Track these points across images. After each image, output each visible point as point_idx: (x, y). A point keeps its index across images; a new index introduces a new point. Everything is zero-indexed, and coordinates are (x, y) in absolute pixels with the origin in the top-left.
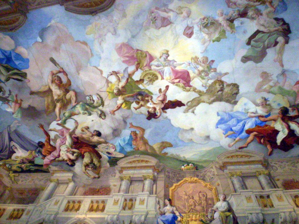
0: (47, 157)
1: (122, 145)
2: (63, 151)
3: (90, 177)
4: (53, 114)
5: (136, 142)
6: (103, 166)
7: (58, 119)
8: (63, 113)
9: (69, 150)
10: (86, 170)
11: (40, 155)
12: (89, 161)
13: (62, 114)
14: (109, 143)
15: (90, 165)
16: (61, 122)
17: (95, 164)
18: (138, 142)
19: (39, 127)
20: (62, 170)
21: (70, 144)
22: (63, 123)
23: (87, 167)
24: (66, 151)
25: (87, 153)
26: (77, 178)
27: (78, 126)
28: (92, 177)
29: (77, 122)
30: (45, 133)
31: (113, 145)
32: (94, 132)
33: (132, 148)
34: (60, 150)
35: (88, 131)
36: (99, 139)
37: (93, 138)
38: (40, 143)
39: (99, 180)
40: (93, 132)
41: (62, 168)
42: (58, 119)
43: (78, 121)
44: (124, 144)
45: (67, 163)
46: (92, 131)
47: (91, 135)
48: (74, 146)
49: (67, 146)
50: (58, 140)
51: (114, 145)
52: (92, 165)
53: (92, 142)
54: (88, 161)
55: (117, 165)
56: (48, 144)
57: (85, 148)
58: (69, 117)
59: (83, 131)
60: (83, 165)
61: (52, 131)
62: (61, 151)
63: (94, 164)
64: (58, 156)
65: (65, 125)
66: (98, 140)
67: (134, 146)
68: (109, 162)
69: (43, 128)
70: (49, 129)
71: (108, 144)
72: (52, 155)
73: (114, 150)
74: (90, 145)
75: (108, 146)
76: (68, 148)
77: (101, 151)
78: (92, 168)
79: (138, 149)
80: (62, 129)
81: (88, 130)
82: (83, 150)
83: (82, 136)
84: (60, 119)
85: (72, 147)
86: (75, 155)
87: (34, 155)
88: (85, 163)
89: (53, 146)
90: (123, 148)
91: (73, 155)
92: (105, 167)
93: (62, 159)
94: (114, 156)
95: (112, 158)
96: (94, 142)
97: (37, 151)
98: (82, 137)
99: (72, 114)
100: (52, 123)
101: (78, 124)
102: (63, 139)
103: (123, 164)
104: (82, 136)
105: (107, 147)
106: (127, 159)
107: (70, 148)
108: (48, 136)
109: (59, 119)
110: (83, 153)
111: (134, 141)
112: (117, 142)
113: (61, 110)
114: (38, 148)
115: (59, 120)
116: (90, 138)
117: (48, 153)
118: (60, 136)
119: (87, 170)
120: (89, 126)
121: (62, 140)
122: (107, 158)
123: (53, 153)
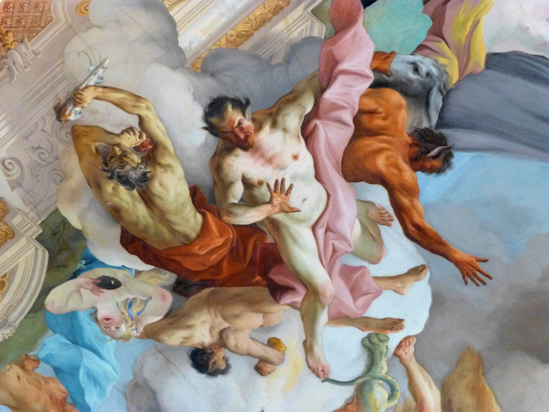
0: (365, 85)
1: (86, 352)
2: (303, 178)
3: (96, 86)
4: (443, 369)
5: (51, 397)
6: (88, 194)
7: (409, 353)
8: (399, 394)
9: (277, 200)
10: (141, 121)
11: (412, 76)
12: (156, 187)
13: (402, 386)
14: (140, 338)
15: (143, 169)
16: (387, 339)
17: (122, 188)
18: (44, 397)
19: (485, 261)
20: (246, 46)
21: (289, 241)
22: (375, 340)
23: (143, 145)
24: (291, 186)
25: (193, 235)
26: (150, 39)
27: (307, 361)
28: (88, 95)
29: (318, 376)
30: (442, 243)
31: (120, 338)
32: (226, 359)
33: (47, 360)
34: (318, 177)
35: (249, 354)
36: (187, 338)
37: (211, 329)
38: (437, 163)
39: (49, 103)
40: (231, 362)
41: (253, 56)
42: (409, 353)
43: (315, 381)
44: (85, 361)
45: (249, 110)
46: (235, 361)
47: (232, 341)
48: (269, 240)
49: (301, 221)
50: (358, 228)
51: (114, 337)
52: (134, 175)
53: (209, 303)
54: (161, 185)
55: (40, 239)
56: (394, 180)
57: (214, 258)
58: (364, 383)
59: (273, 343)
60: (171, 148)
61: (404, 270)
62: (312, 172)
63: (125, 181)
64: (315, 127)
65: (365, 334)
66: (190, 327)
67: (44, 370)
68: (79, 235)
69: (457, 263)
70: (427, 276)
71: (141, 329)
72: (348, 117)
73: (101, 315)
74: (204, 284)
75: (136, 321)
76: (289, 210)
77: (143, 277)
78: (124, 154)
79: (23, 367)
80: (367, 305)
81: (256, 361)
82: (219, 242)
83: (265, 314)
84: (395, 354)
85: (274, 224)
86: (238, 190)
87: (443, 45)
88: (169, 166)
89: (363, 185)
90: (75, 342)
91: (248, 184)
92: (73, 197)
93: (280, 119)
94: (80, 280)
95: (82, 264)
96: (198, 307)
97: (435, 91)
98: (257, 312)
99: (358, 404)
100: (425, 316)
101: (310, 367)
102: (334, 251)
103: (21, 261)
104: (265, 313)
105: (135, 310)
106: (26, 300)
107: (280, 217)
108: (418, 228)
109: (401, 352)
110: (209, 216)
111: (59, 395)
112: (113, 359)
113: (413, 404)
114: (442, 123)
115: (399, 347)
116: (226, 325)
117: (372, 112)
118: (356, 262)
119: (134, 122)
120: (261, 381)
121: (339, 244)
122: (100, 254)
123: (349, 132)
